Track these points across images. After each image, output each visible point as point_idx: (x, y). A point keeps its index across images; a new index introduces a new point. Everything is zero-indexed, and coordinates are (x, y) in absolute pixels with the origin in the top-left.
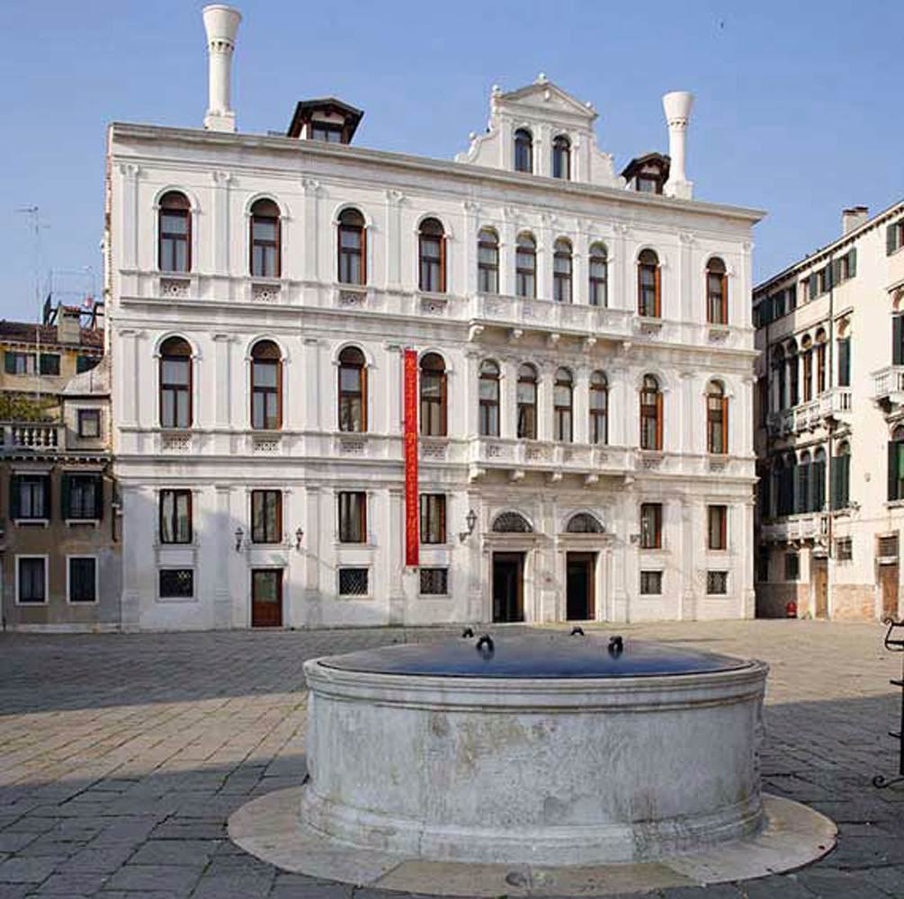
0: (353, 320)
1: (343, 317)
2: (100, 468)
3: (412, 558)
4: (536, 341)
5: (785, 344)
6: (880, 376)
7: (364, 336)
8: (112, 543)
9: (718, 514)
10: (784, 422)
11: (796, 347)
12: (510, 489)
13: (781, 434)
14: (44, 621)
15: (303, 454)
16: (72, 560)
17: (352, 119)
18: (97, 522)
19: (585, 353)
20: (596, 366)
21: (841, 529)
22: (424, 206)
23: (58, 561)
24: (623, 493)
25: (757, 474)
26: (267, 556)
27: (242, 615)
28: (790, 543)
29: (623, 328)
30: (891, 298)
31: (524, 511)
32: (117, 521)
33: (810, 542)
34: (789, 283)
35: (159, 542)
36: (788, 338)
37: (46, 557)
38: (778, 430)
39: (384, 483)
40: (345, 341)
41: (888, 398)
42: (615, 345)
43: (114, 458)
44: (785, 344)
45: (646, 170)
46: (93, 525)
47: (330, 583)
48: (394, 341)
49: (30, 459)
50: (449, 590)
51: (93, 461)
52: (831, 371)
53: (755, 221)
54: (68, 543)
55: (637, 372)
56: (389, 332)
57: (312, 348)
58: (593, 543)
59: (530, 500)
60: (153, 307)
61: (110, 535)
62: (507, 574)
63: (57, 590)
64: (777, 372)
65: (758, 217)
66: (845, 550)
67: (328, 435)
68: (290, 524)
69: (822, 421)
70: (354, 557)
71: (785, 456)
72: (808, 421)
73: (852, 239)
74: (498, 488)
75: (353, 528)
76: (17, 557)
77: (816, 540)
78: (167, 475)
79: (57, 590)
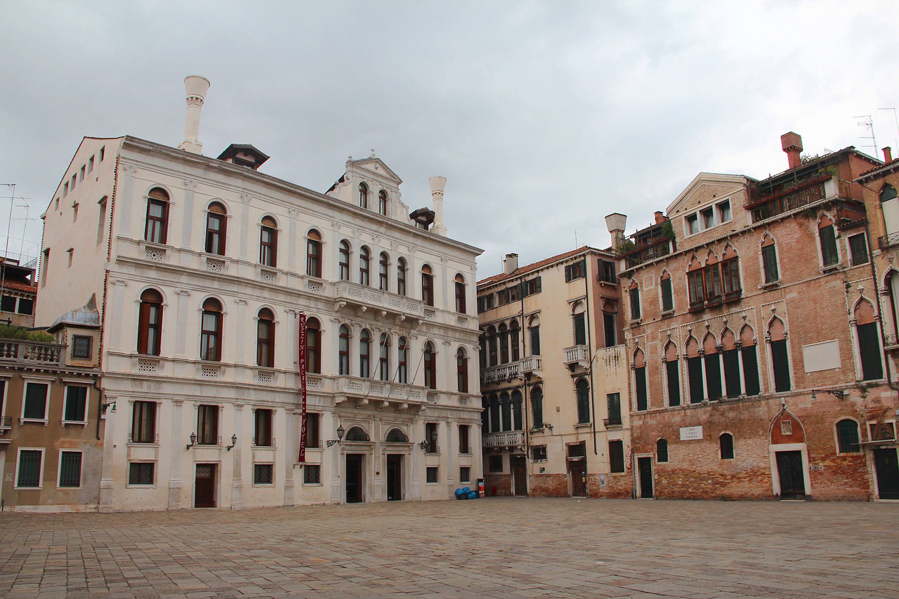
0: (269, 289)
1: (262, 288)
3: (302, 459)
4: (371, 316)
6: (569, 350)
7: (274, 301)
8: (96, 441)
11: (496, 330)
12: (356, 411)
14: (36, 503)
17: (261, 158)
19: (396, 325)
21: (537, 441)
22: (307, 222)
23: (52, 453)
24: (417, 417)
25: (483, 406)
26: (207, 454)
27: (188, 497)
28: (496, 449)
29: (418, 312)
30: (571, 306)
31: (364, 426)
32: (101, 423)
33: (512, 448)
34: (487, 293)
35: (131, 441)
37: (43, 450)
41: (578, 363)
42: (412, 322)
43: (103, 375)
47: (248, 473)
48: (292, 307)
49: (38, 371)
50: (321, 480)
51: (87, 376)
52: (524, 346)
54: (62, 439)
56: (288, 301)
57: (242, 306)
58: (401, 448)
59: (367, 419)
60: (138, 265)
61: (95, 434)
63: (50, 478)
66: (540, 453)
70: (264, 456)
73: (538, 272)
74: (349, 410)
75: (264, 437)
76: (19, 449)
78: (140, 390)
79: (50, 478)
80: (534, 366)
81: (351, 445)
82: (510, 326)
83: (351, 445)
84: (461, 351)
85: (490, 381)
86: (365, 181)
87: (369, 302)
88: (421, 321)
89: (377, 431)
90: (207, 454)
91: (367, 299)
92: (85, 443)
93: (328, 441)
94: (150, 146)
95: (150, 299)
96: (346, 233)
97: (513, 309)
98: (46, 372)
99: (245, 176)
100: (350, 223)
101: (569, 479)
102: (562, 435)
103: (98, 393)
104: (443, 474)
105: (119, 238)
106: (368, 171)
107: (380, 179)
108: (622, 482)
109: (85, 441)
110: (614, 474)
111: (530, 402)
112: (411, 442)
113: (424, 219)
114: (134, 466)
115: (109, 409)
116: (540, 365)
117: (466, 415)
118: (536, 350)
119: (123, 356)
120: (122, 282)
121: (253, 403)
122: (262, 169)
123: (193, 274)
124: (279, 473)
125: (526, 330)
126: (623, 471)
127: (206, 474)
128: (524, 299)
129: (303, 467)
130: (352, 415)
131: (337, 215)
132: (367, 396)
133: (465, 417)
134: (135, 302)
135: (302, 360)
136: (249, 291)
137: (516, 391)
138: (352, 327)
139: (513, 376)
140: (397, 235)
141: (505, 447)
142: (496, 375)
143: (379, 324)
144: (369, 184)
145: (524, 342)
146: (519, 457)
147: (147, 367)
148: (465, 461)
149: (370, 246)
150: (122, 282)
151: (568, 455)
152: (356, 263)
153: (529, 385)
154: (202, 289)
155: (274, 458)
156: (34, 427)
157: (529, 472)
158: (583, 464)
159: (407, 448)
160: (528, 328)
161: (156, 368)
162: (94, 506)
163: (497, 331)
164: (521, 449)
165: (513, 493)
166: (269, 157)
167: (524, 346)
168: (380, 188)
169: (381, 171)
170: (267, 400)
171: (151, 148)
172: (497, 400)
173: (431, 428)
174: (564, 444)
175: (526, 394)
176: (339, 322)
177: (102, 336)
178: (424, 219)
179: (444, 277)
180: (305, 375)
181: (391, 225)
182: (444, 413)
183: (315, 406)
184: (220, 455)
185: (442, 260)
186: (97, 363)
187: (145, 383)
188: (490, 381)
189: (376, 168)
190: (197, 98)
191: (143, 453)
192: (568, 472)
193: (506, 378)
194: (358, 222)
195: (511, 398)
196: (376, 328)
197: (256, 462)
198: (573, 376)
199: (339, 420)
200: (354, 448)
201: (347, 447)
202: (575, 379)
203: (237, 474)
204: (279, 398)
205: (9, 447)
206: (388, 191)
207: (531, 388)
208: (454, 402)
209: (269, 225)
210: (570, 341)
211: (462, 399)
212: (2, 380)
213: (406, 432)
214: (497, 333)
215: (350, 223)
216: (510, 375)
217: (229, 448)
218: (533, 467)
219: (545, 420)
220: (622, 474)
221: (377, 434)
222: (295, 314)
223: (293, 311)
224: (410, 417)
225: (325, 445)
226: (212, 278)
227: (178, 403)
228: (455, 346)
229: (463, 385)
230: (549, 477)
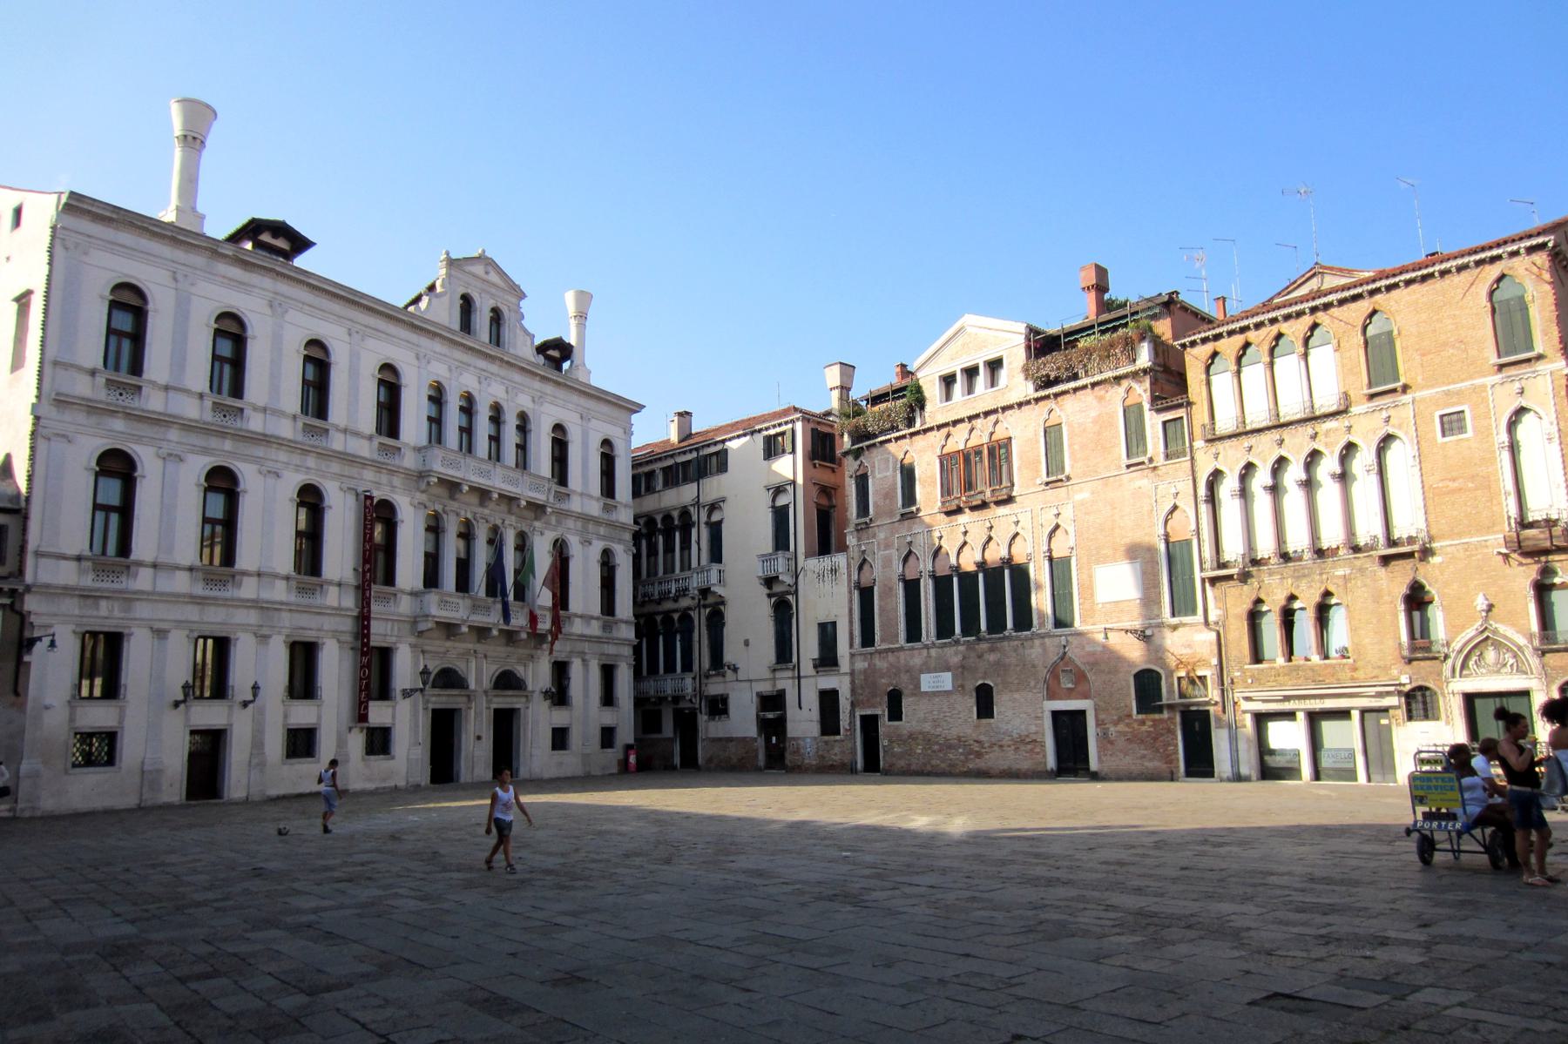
0: (315, 455)
1: (305, 452)
6: (765, 559)
8: (12, 698)
15: (253, 596)
17: (300, 244)
21: (714, 688)
24: (539, 652)
25: (636, 637)
26: (209, 715)
27: (173, 787)
32: (22, 669)
33: (677, 699)
34: (647, 469)
35: (77, 697)
39: (335, 634)
40: (304, 477)
42: (537, 509)
43: (28, 589)
47: (275, 744)
48: (352, 484)
55: (550, 536)
57: (271, 481)
58: (515, 700)
59: (465, 655)
60: (91, 408)
62: (444, 728)
66: (719, 706)
67: (276, 576)
70: (303, 714)
72: (673, 591)
74: (437, 642)
75: (303, 683)
77: (688, 698)
80: (714, 578)
81: (439, 695)
83: (439, 695)
84: (607, 555)
86: (469, 291)
87: (473, 478)
88: (549, 510)
89: (479, 673)
90: (209, 715)
91: (469, 472)
93: (404, 690)
94: (113, 212)
95: (114, 465)
96: (439, 371)
97: (685, 494)
99: (279, 274)
100: (445, 355)
101: (761, 742)
102: (751, 681)
103: (17, 618)
104: (575, 738)
105: (56, 363)
106: (474, 276)
107: (493, 290)
108: (837, 750)
110: (826, 738)
113: (555, 353)
114: (86, 737)
115: (40, 648)
118: (716, 555)
119: (64, 557)
120: (63, 436)
121: (286, 631)
122: (301, 261)
123: (188, 427)
125: (703, 526)
126: (839, 734)
128: (701, 481)
129: (365, 731)
130: (442, 650)
131: (425, 342)
132: (465, 621)
133: (610, 652)
134: (86, 469)
135: (368, 566)
136: (283, 456)
137: (686, 616)
138: (445, 516)
140: (517, 377)
141: (666, 698)
142: (655, 591)
143: (486, 511)
144: (475, 296)
145: (699, 544)
148: (608, 717)
149: (475, 394)
150: (63, 436)
152: (453, 419)
153: (705, 606)
154: (205, 451)
155: (319, 717)
157: (701, 735)
158: (781, 723)
159: (524, 700)
160: (707, 523)
161: (123, 578)
163: (659, 526)
164: (691, 701)
166: (314, 244)
168: (492, 303)
169: (493, 277)
170: (309, 627)
171: (114, 216)
173: (561, 670)
174: (754, 695)
175: (700, 619)
176: (426, 507)
178: (555, 353)
180: (370, 590)
181: (508, 363)
182: (580, 646)
183: (385, 635)
184: (230, 715)
185: (582, 418)
186: (15, 569)
187: (103, 603)
189: (487, 273)
190: (194, 138)
191: (99, 716)
192: (760, 734)
194: (458, 354)
195: (677, 625)
196: (482, 518)
198: (770, 596)
199: (421, 657)
200: (444, 699)
201: (434, 699)
202: (773, 600)
203: (258, 744)
204: (329, 623)
206: (505, 309)
207: (708, 610)
208: (595, 629)
209: (316, 353)
210: (767, 545)
211: (607, 627)
214: (659, 530)
215: (445, 355)
217: (245, 704)
218: (709, 728)
219: (728, 657)
220: (838, 737)
221: (479, 681)
222: (357, 495)
223: (353, 489)
224: (527, 652)
225: (398, 694)
226: (222, 434)
227: (160, 634)
228: (598, 546)
229: (608, 606)
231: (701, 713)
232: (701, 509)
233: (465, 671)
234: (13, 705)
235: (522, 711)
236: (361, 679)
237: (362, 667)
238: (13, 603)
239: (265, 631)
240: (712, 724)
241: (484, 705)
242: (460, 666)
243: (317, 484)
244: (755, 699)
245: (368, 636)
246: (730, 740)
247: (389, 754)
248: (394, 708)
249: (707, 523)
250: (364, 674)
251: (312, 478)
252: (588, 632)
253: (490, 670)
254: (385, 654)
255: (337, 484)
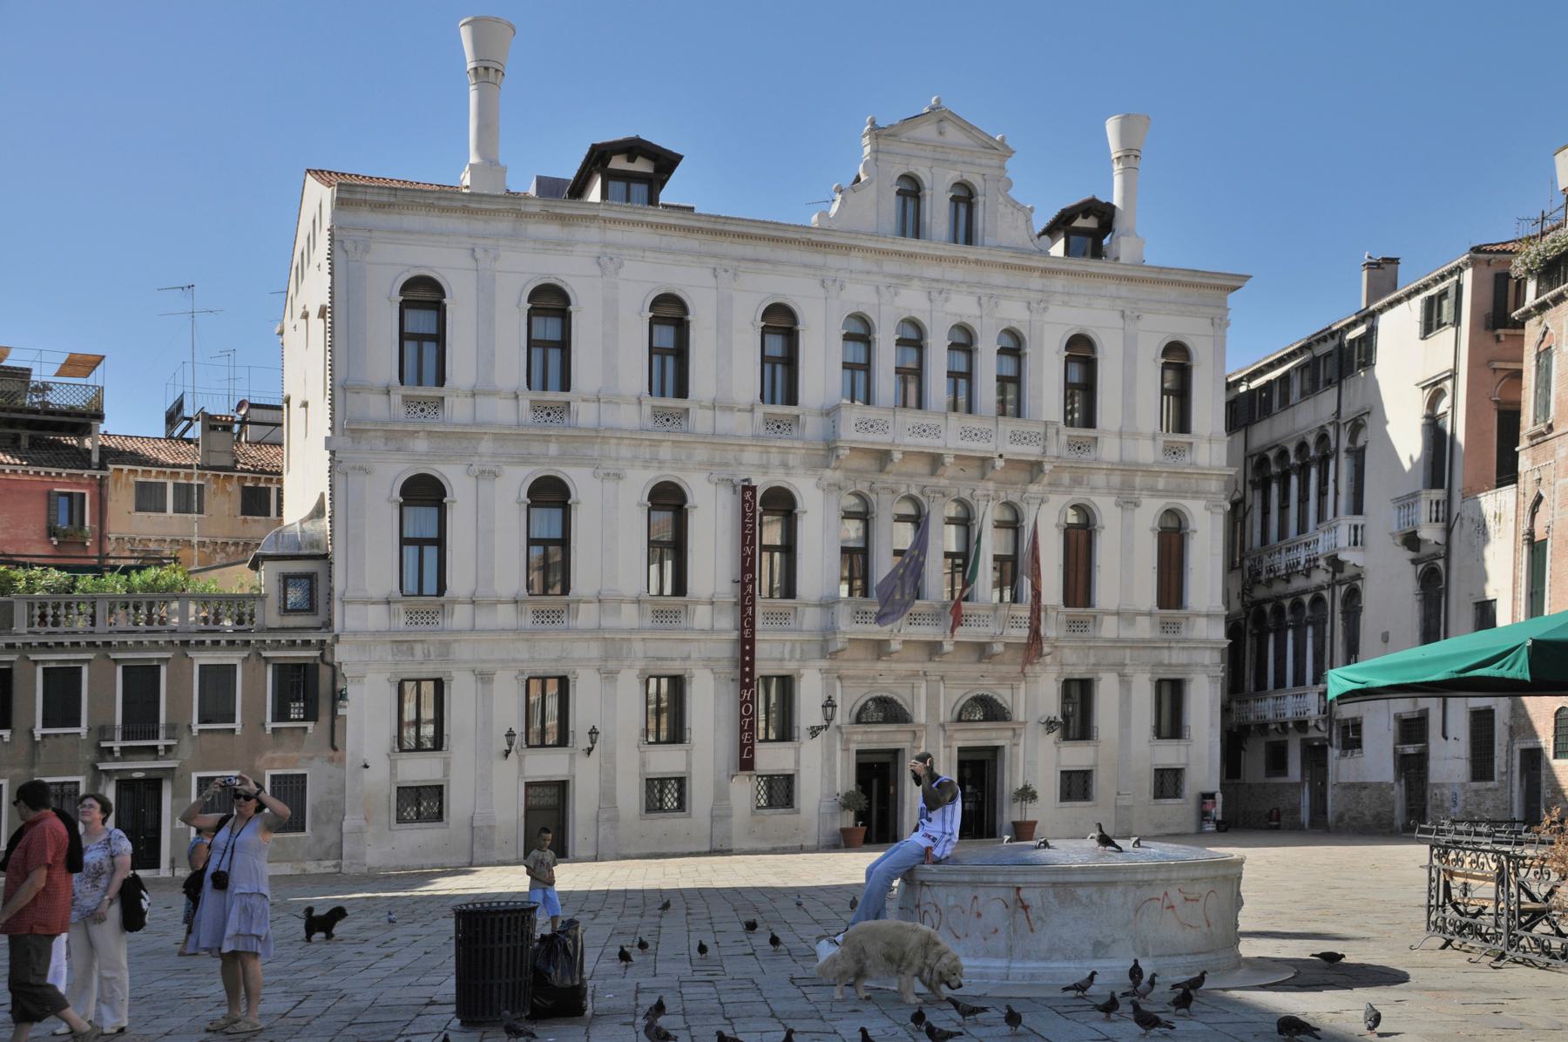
2: (317, 653)
5: (1272, 455)
8: (332, 753)
9: (1171, 694)
10: (1267, 562)
11: (1289, 457)
13: (1264, 577)
16: (273, 777)
18: (310, 725)
20: (1003, 497)
26: (548, 765)
28: (1273, 727)
36: (1277, 446)
38: (1259, 573)
44: (1272, 455)
45: (1080, 223)
46: (305, 729)
49: (216, 643)
51: (307, 643)
53: (1234, 289)
54: (269, 754)
64: (1258, 495)
65: (1235, 284)
68: (580, 721)
69: (1322, 563)
70: (667, 761)
71: (1268, 608)
72: (1303, 562)
74: (862, 665)
76: (195, 776)
77: (1311, 723)
80: (1343, 536)
82: (1317, 448)
83: (866, 732)
85: (1272, 575)
90: (548, 765)
92: (311, 759)
98: (231, 643)
101: (1398, 793)
109: (310, 755)
110: (1476, 785)
111: (1341, 622)
112: (1022, 719)
116: (1359, 539)
117: (1177, 657)
124: (700, 795)
125: (1343, 455)
126: (1492, 778)
127: (549, 798)
128: (1344, 382)
133: (1174, 661)
137: (1318, 600)
139: (1312, 564)
142: (1281, 561)
145: (1336, 481)
146: (1316, 744)
147: (422, 618)
151: (1398, 741)
153: (1340, 583)
156: (218, 737)
157: (1331, 779)
158: (1421, 760)
160: (1348, 451)
162: (334, 862)
165: (1304, 825)
167: (1337, 493)
172: (1284, 617)
174: (1392, 717)
175: (1335, 601)
177: (330, 571)
179: (1129, 358)
180: (753, 606)
182: (1114, 656)
183: (782, 660)
188: (1272, 575)
192: (1398, 779)
193: (1300, 568)
195: (1308, 613)
197: (648, 774)
198: (1414, 562)
200: (875, 737)
201: (859, 737)
202: (1420, 567)
203: (607, 795)
205: (177, 773)
207: (1344, 588)
212: (155, 663)
213: (1010, 704)
216: (1306, 561)
217: (590, 751)
218: (1342, 768)
222: (734, 486)
227: (484, 678)
229: (1171, 589)
230: (1365, 788)
231: (1331, 746)
232: (1342, 428)
233: (909, 700)
234: (331, 760)
235: (1007, 751)
236: (742, 717)
237: (742, 704)
238: (322, 655)
239: (612, 665)
240: (1344, 761)
241: (942, 744)
242: (900, 694)
243: (676, 481)
244: (1393, 724)
245: (751, 664)
246: (1363, 786)
247: (792, 807)
248: (798, 751)
249: (1348, 451)
250: (747, 708)
251: (668, 474)
252: (1128, 633)
253: (952, 697)
254: (787, 684)
255: (704, 475)
